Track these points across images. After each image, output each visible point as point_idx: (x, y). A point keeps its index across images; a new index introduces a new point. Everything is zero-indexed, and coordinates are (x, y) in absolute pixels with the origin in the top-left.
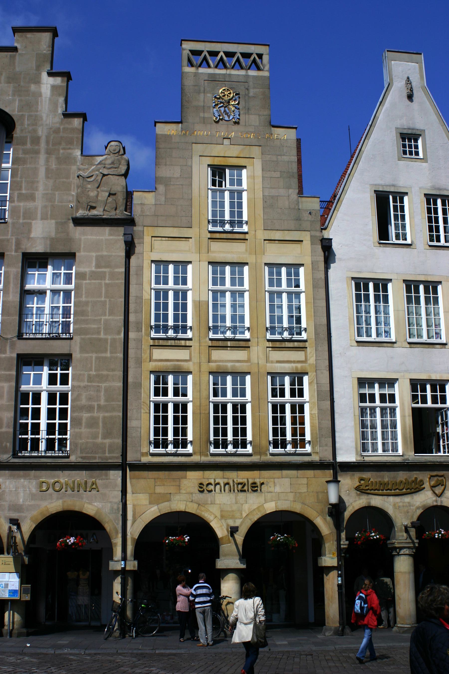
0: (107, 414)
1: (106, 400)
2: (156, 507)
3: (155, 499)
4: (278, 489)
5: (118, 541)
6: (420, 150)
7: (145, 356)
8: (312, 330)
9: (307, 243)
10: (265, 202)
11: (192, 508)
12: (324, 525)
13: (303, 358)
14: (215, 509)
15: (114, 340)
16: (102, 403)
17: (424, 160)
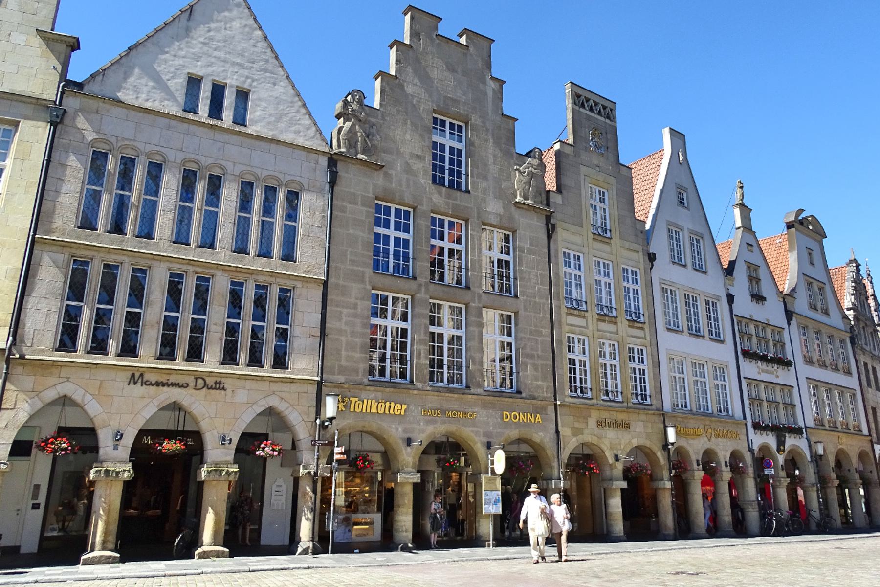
0: (544, 363)
1: (542, 351)
2: (574, 439)
3: (576, 432)
4: (638, 430)
5: (555, 464)
6: (685, 201)
7: (563, 320)
8: (646, 315)
9: (641, 254)
10: (619, 219)
11: (595, 440)
12: (661, 456)
13: (643, 335)
14: (607, 442)
15: (544, 304)
16: (540, 353)
17: (688, 209)
